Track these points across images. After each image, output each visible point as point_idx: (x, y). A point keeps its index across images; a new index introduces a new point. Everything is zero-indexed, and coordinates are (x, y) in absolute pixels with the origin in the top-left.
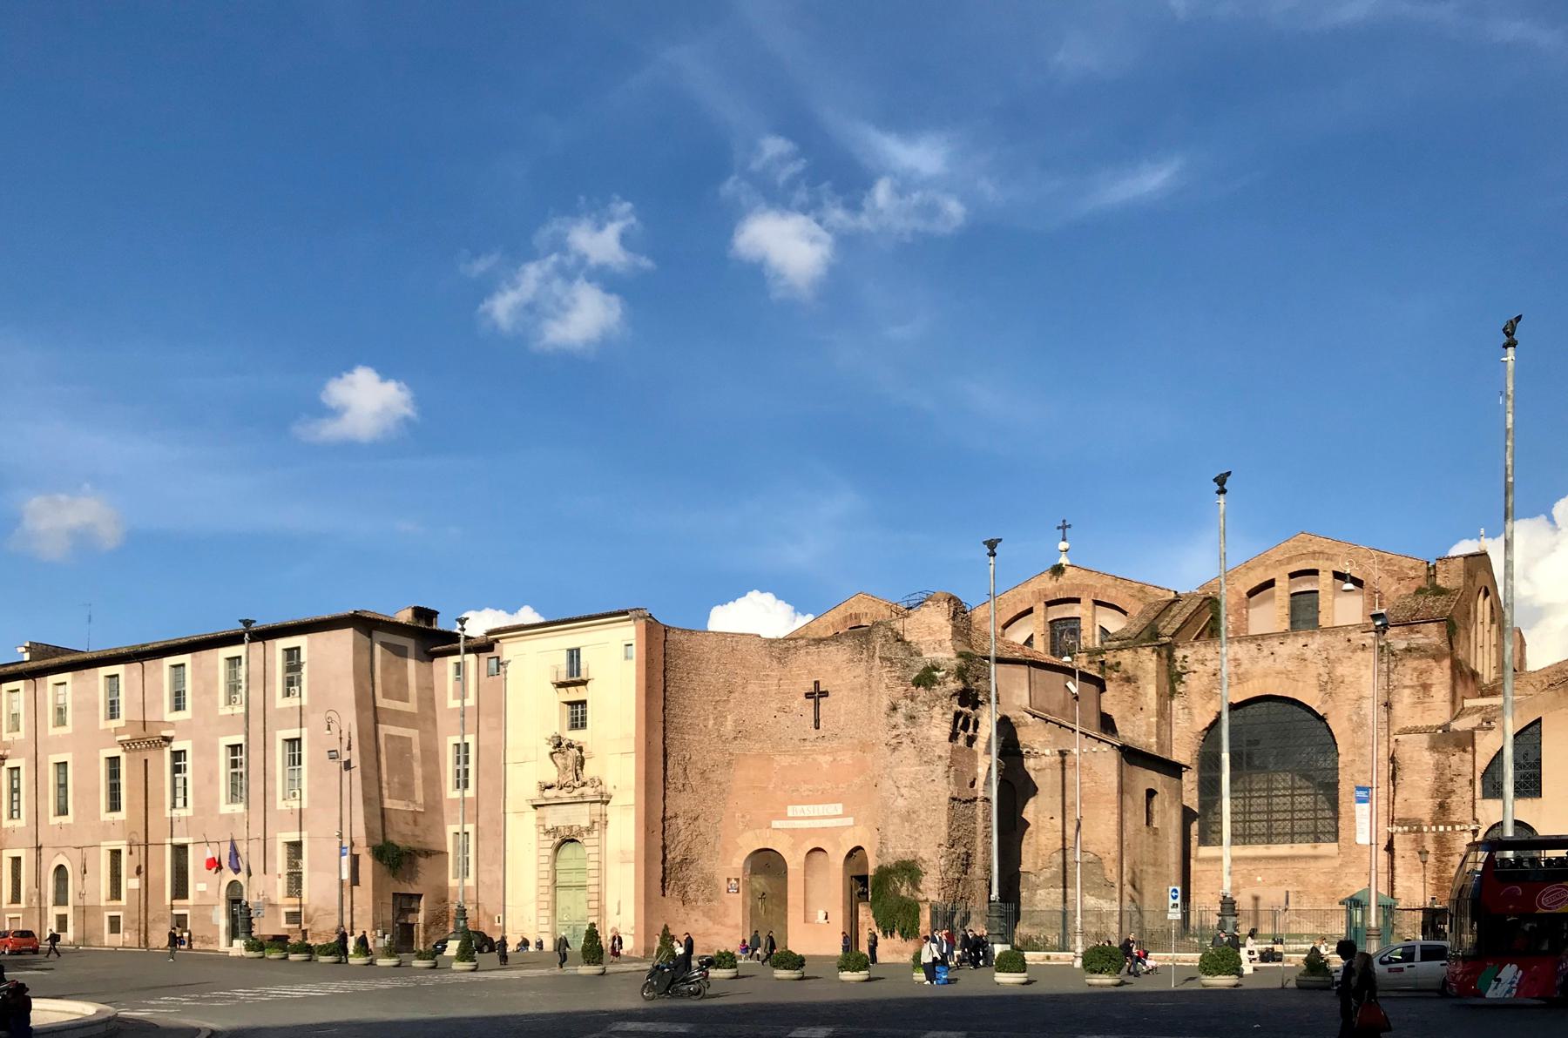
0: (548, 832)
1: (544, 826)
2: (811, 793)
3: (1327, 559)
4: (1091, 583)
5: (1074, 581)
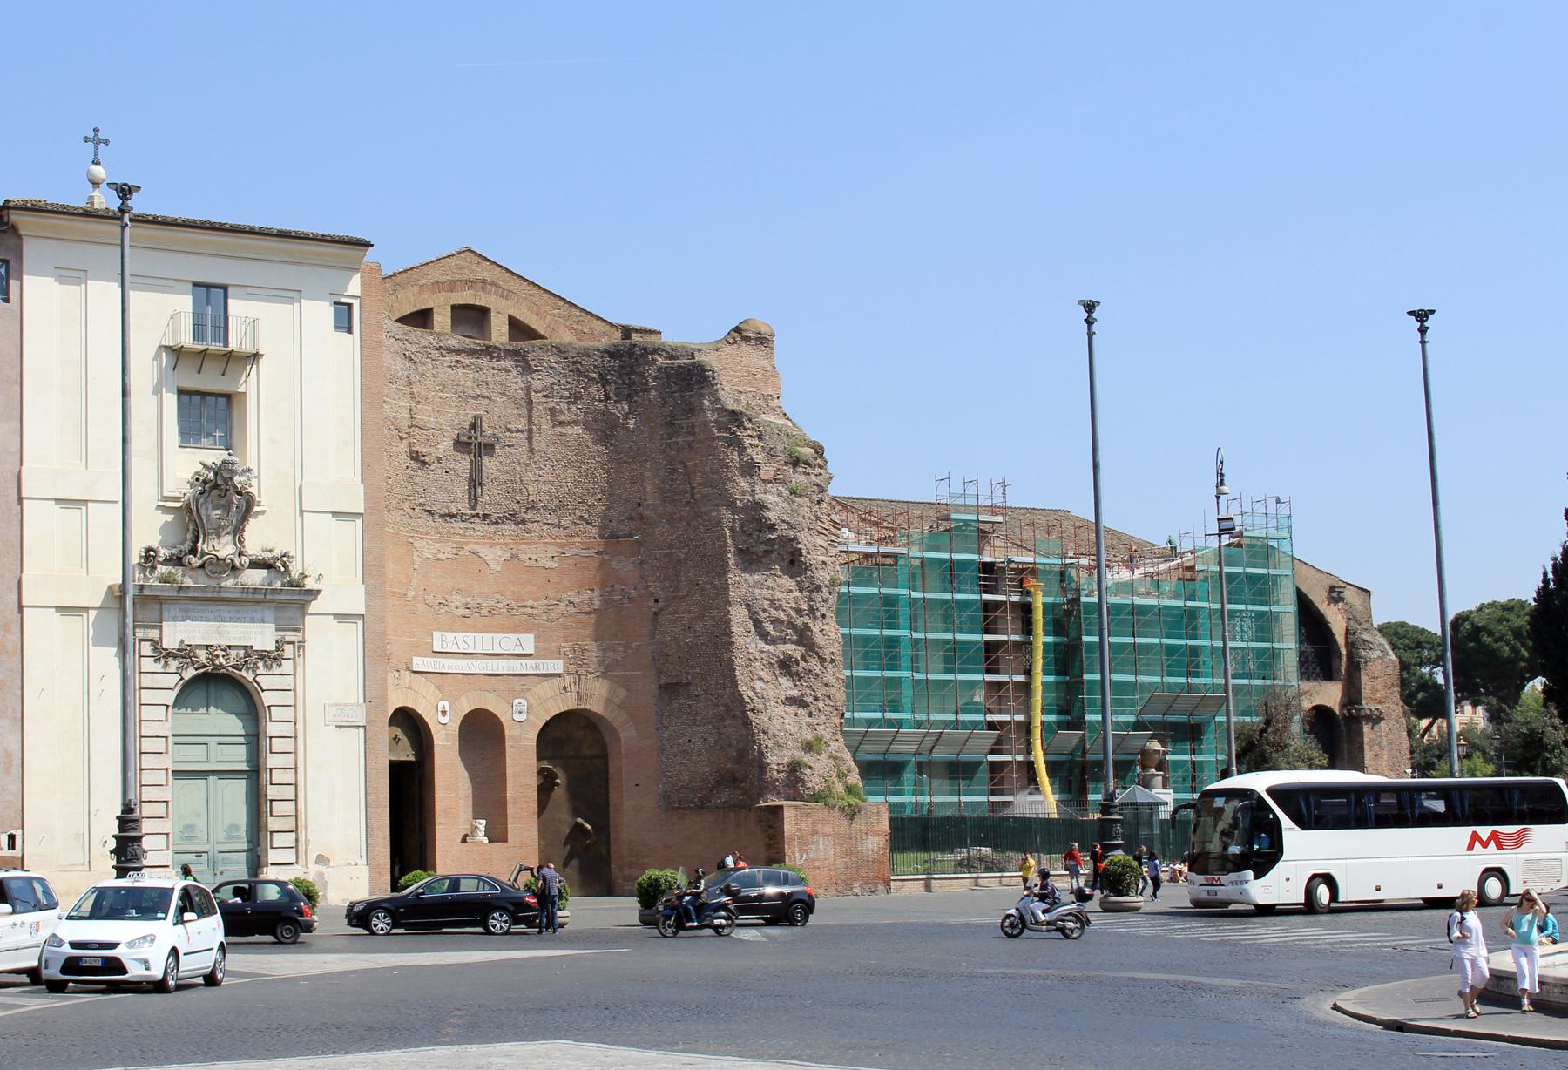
0: (168, 654)
1: (156, 644)
2: (467, 612)
3: (502, 296)
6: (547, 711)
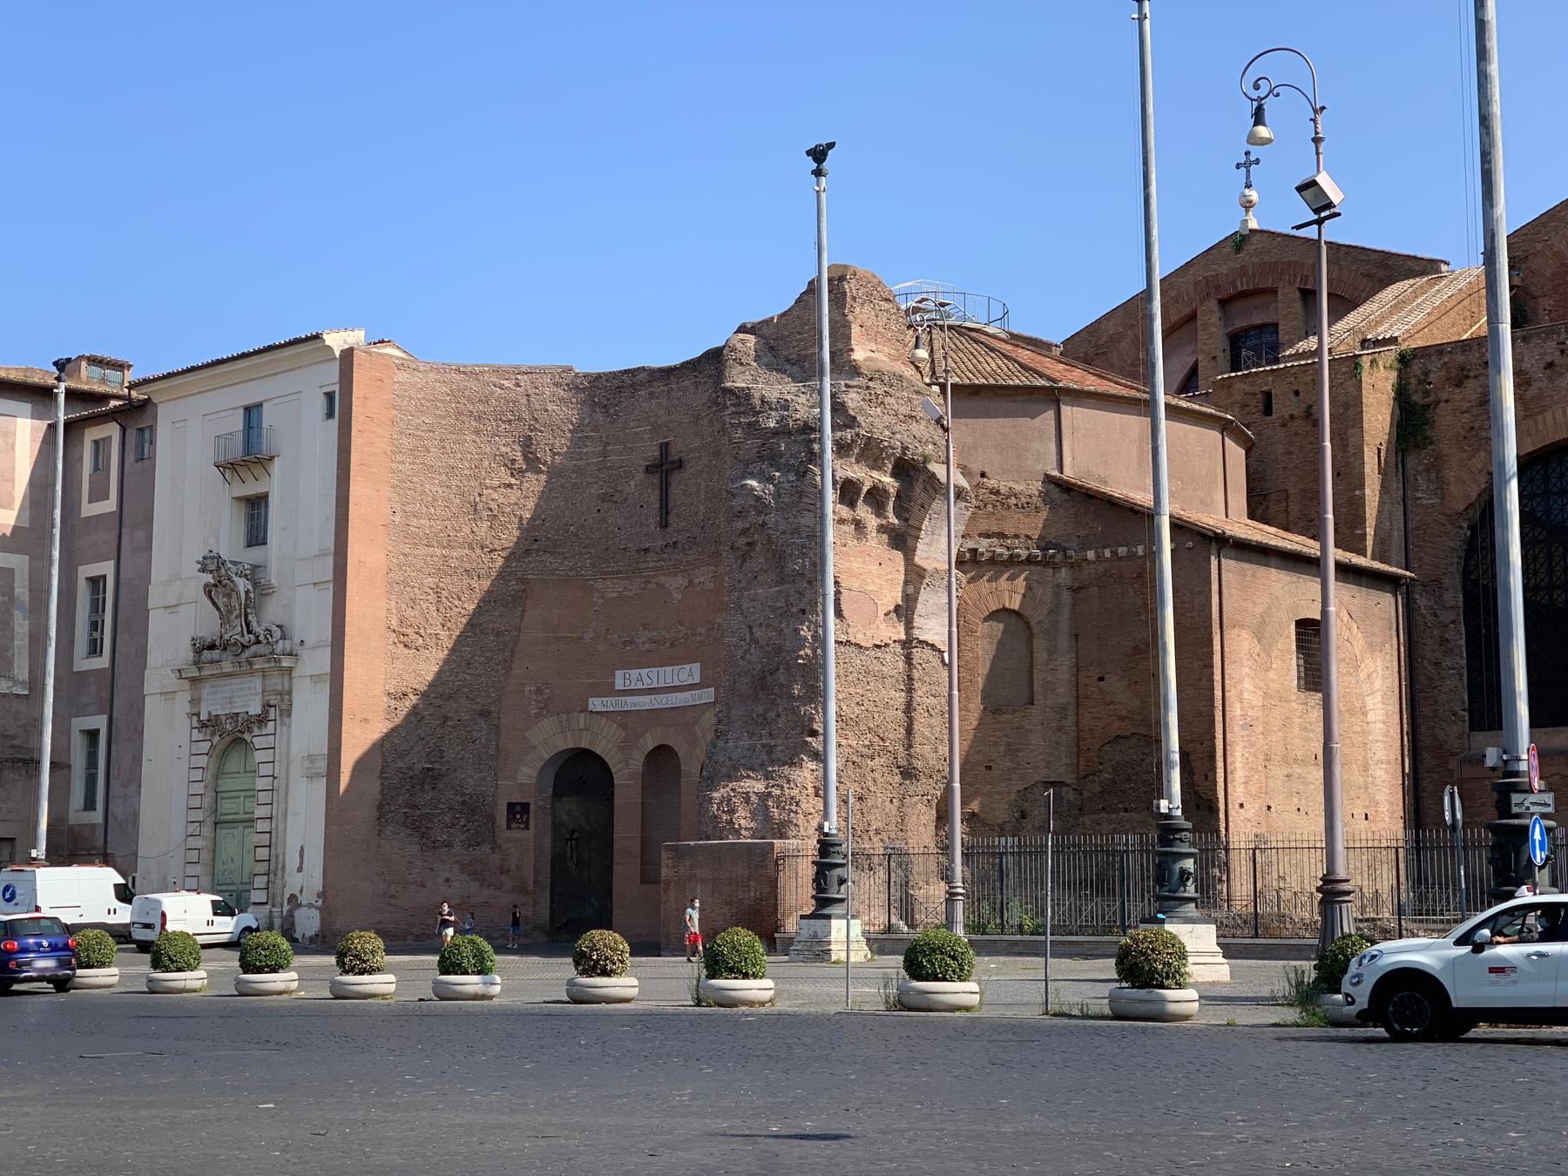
1: (198, 715)
4: (1292, 259)
5: (1266, 258)
6: (574, 743)
